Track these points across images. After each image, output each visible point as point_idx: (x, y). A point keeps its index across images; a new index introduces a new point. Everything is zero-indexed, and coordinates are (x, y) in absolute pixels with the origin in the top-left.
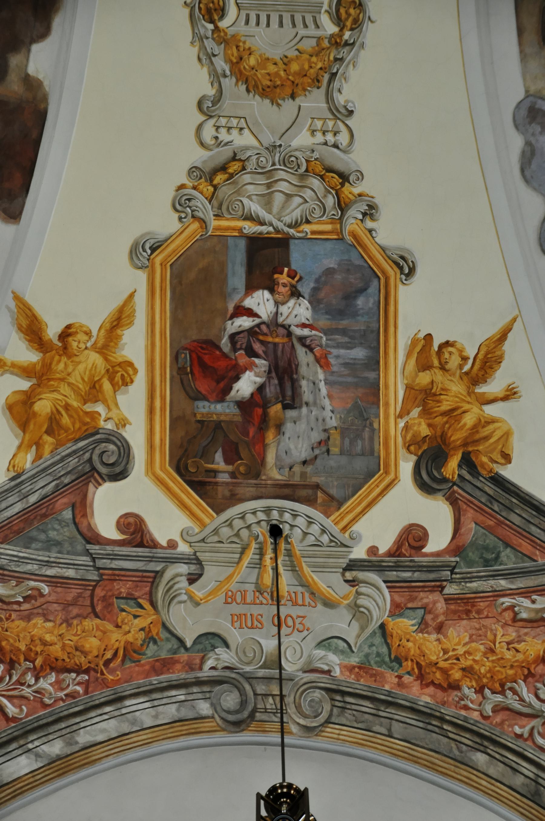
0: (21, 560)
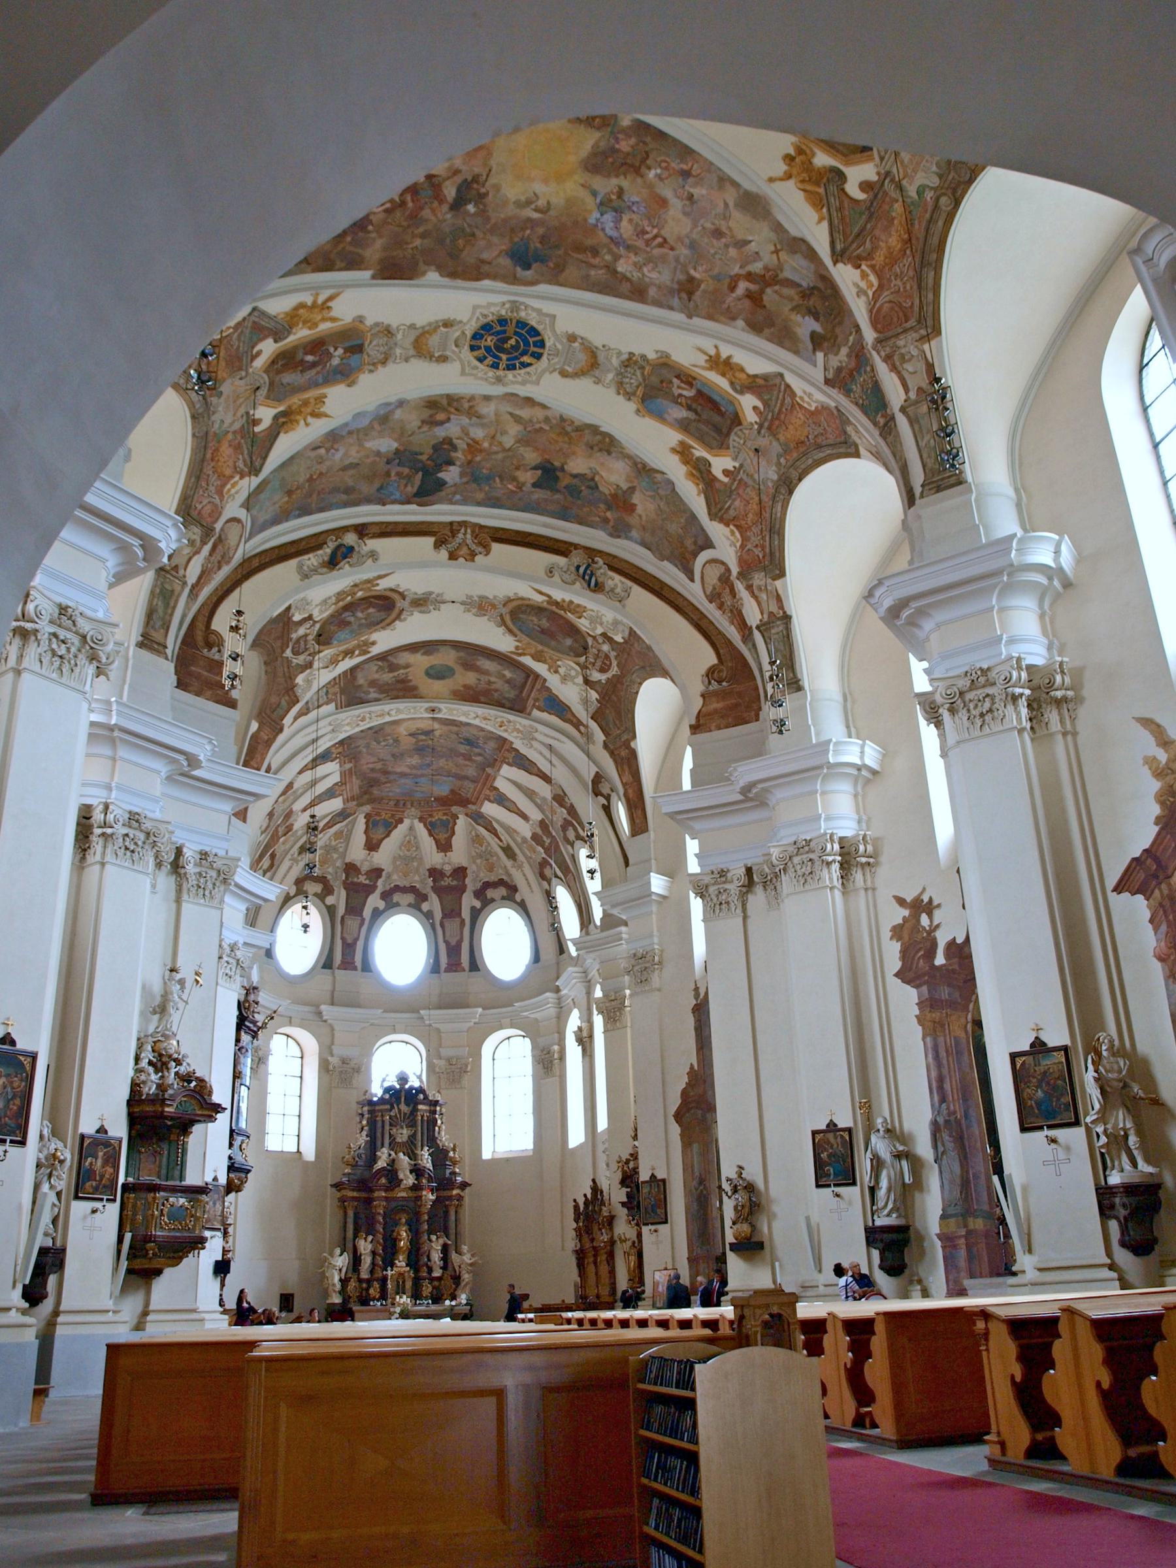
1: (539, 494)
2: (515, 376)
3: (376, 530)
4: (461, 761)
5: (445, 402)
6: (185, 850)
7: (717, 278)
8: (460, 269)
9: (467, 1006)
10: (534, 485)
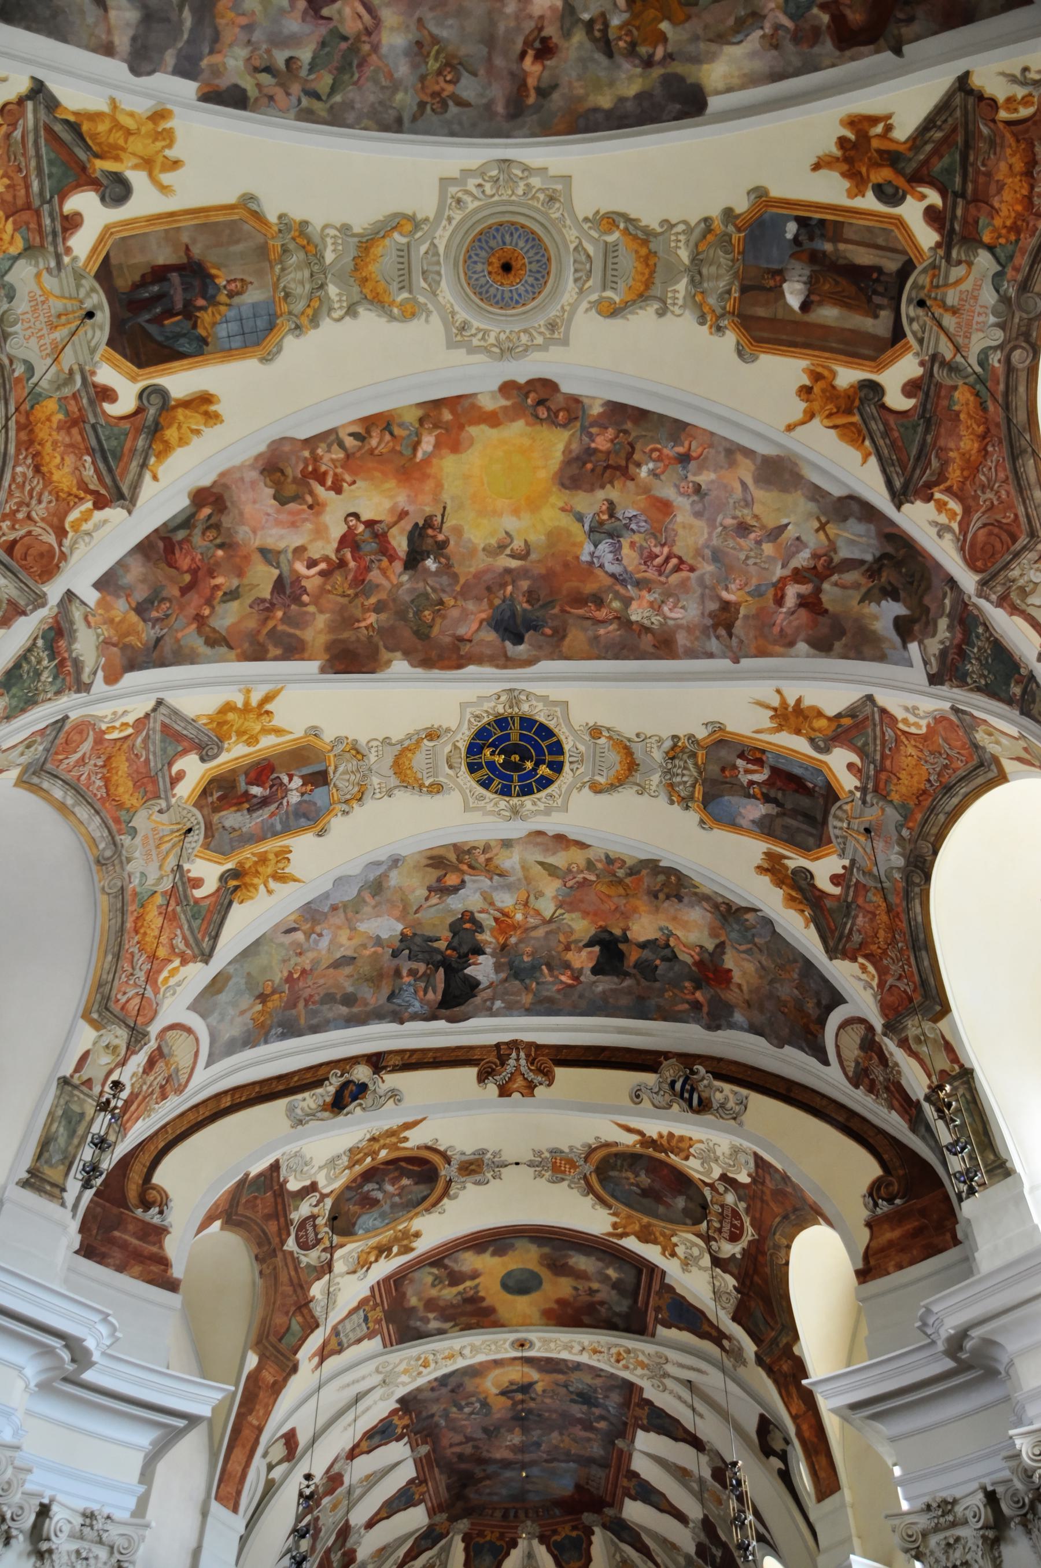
0: (154, 743)
1: (604, 984)
2: (534, 804)
3: (397, 1060)
4: (579, 1432)
5: (452, 857)
6: (55, 1508)
7: (758, 593)
8: (434, 654)
10: (595, 971)
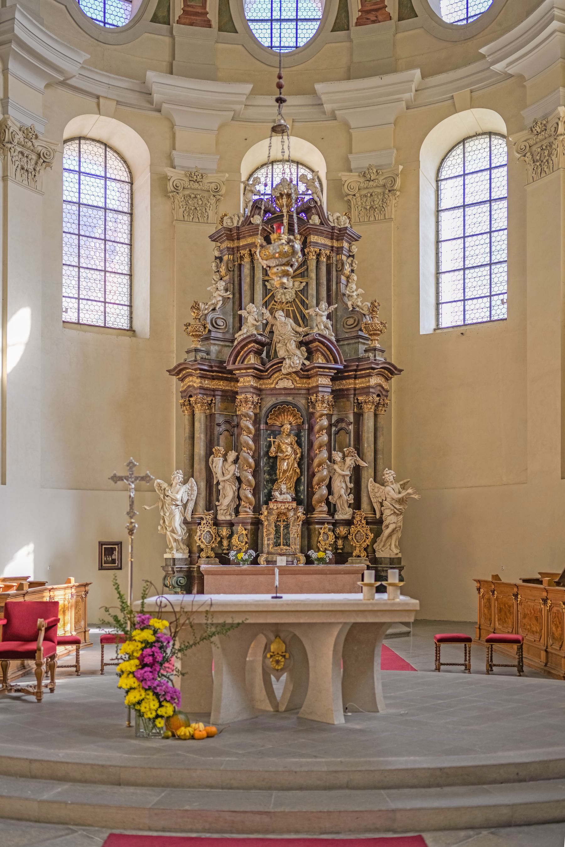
9: (393, 69)
